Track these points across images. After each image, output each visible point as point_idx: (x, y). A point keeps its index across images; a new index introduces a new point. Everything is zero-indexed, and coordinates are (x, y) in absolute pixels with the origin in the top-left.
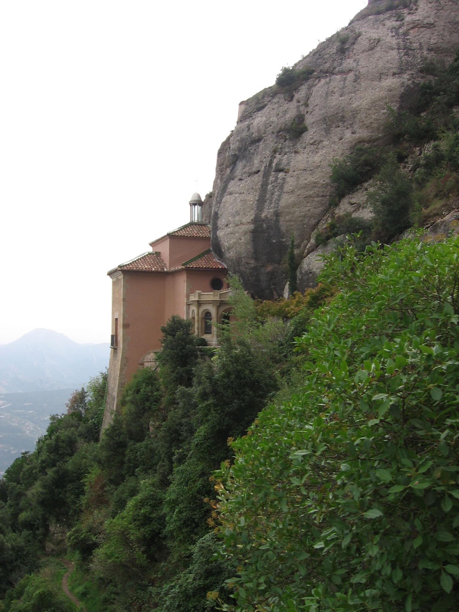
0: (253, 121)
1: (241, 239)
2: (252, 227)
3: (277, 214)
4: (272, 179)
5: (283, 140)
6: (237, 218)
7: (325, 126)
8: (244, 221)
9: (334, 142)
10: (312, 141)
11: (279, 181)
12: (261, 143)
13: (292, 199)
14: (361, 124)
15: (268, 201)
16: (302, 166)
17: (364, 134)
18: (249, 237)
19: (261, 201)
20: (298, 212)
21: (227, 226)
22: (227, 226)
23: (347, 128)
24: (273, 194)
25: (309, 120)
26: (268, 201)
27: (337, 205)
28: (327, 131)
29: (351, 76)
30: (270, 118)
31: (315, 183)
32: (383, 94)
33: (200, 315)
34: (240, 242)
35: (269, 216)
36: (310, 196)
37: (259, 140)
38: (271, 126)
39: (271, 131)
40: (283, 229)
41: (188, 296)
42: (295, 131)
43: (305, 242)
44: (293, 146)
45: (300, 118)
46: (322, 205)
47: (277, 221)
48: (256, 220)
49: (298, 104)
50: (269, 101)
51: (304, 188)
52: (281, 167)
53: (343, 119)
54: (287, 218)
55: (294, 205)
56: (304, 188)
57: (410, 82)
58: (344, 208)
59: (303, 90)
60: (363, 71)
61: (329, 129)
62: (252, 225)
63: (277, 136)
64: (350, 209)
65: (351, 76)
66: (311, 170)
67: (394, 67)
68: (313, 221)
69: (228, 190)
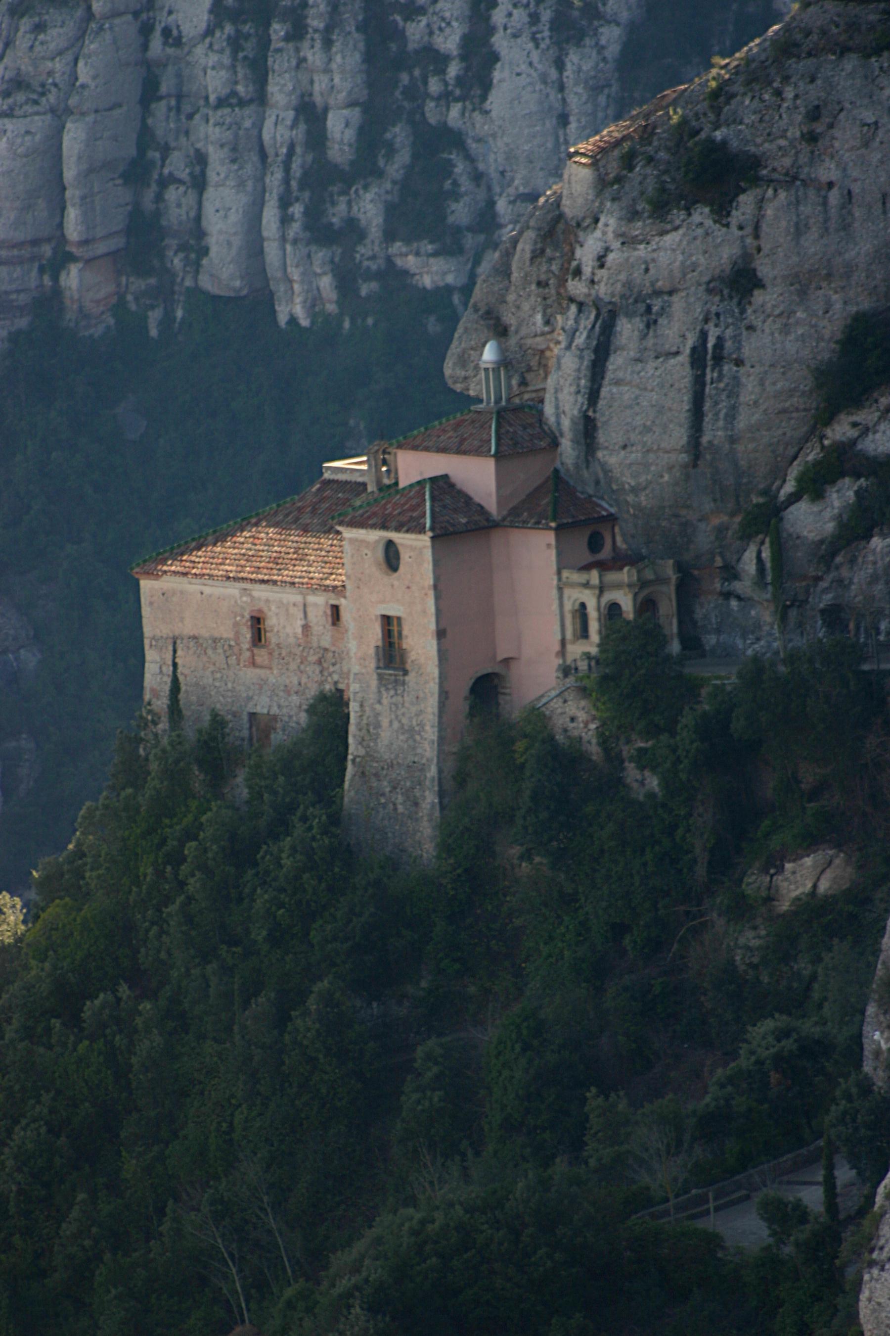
0: (655, 255)
1: (662, 476)
5: (717, 298)
6: (648, 438)
7: (797, 286)
10: (777, 312)
12: (675, 298)
21: (625, 447)
22: (625, 447)
24: (716, 403)
25: (764, 269)
26: (710, 415)
28: (803, 293)
29: (834, 198)
30: (691, 255)
33: (602, 610)
34: (661, 481)
35: (716, 442)
37: (671, 293)
38: (693, 271)
41: (559, 573)
42: (741, 282)
43: (778, 483)
45: (747, 257)
49: (740, 233)
50: (683, 221)
54: (751, 446)
58: (840, 430)
59: (746, 201)
62: (683, 455)
63: (709, 291)
66: (783, 367)
68: (792, 451)
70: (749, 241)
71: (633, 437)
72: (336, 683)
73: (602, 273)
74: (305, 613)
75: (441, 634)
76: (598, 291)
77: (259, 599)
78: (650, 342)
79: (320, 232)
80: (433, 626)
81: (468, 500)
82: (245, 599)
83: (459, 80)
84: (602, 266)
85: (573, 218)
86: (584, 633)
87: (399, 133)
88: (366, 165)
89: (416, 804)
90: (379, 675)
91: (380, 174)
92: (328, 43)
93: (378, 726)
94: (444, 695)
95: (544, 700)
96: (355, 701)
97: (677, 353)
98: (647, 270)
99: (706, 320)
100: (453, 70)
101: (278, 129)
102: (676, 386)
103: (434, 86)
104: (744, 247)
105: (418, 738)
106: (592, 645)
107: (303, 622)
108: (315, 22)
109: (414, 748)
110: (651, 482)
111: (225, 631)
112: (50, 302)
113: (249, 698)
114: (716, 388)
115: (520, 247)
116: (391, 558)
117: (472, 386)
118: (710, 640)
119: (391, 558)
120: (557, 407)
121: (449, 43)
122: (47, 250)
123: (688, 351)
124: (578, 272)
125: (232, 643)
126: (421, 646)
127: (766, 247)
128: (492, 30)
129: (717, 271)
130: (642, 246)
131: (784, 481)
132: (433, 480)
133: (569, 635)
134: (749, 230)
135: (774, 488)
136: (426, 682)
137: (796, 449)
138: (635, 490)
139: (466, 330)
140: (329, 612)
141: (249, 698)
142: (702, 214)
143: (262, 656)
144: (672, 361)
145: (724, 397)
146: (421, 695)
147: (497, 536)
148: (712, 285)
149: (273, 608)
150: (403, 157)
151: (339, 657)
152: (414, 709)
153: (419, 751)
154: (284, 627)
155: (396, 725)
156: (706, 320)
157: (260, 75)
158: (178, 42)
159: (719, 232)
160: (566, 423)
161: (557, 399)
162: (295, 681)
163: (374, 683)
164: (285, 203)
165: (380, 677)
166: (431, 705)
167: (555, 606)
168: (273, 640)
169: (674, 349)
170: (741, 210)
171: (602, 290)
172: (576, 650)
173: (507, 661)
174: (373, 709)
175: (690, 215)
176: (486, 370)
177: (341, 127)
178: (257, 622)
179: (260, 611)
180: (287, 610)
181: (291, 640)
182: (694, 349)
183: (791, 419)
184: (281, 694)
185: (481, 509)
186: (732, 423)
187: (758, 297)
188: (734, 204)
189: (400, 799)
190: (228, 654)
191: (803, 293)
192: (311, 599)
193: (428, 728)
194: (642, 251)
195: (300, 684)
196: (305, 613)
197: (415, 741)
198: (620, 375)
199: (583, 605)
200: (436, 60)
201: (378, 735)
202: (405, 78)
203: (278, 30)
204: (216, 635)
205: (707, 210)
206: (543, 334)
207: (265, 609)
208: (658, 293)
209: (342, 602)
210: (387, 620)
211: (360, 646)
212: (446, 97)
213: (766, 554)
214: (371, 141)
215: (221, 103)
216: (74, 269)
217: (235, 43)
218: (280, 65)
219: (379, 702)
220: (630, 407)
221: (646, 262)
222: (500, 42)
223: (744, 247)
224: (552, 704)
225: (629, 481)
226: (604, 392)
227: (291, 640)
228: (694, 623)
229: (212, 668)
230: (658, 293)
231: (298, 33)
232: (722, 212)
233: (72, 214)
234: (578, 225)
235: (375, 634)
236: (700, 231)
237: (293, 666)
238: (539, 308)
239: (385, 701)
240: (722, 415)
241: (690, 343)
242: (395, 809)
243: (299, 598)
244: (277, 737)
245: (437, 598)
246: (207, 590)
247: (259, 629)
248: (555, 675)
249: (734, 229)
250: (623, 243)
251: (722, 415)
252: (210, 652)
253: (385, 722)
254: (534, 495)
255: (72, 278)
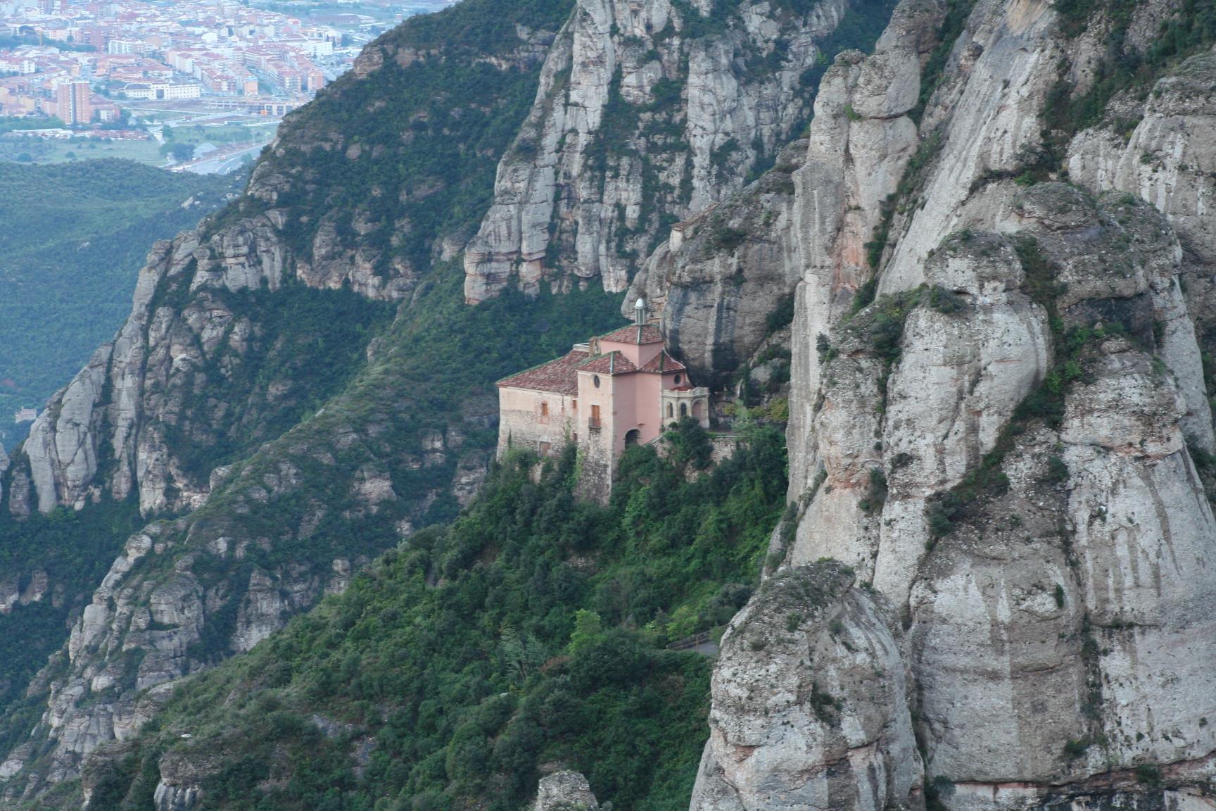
79: (621, 254)
81: (627, 361)
83: (679, 197)
87: (654, 216)
88: (639, 230)
91: (646, 231)
92: (628, 181)
100: (677, 192)
101: (607, 212)
103: (669, 198)
108: (623, 173)
112: (515, 277)
116: (597, 382)
119: (597, 382)
121: (676, 181)
122: (515, 257)
128: (692, 177)
147: (639, 377)
150: (656, 225)
151: (576, 421)
157: (601, 191)
158: (569, 177)
164: (608, 242)
177: (632, 212)
178: (544, 405)
185: (633, 365)
191: (762, 285)
200: (669, 188)
202: (657, 194)
203: (609, 174)
211: (583, 417)
212: (674, 202)
214: (643, 218)
215: (585, 202)
216: (525, 264)
217: (591, 179)
218: (610, 187)
222: (696, 182)
231: (616, 176)
233: (524, 244)
254: (653, 362)
255: (524, 268)
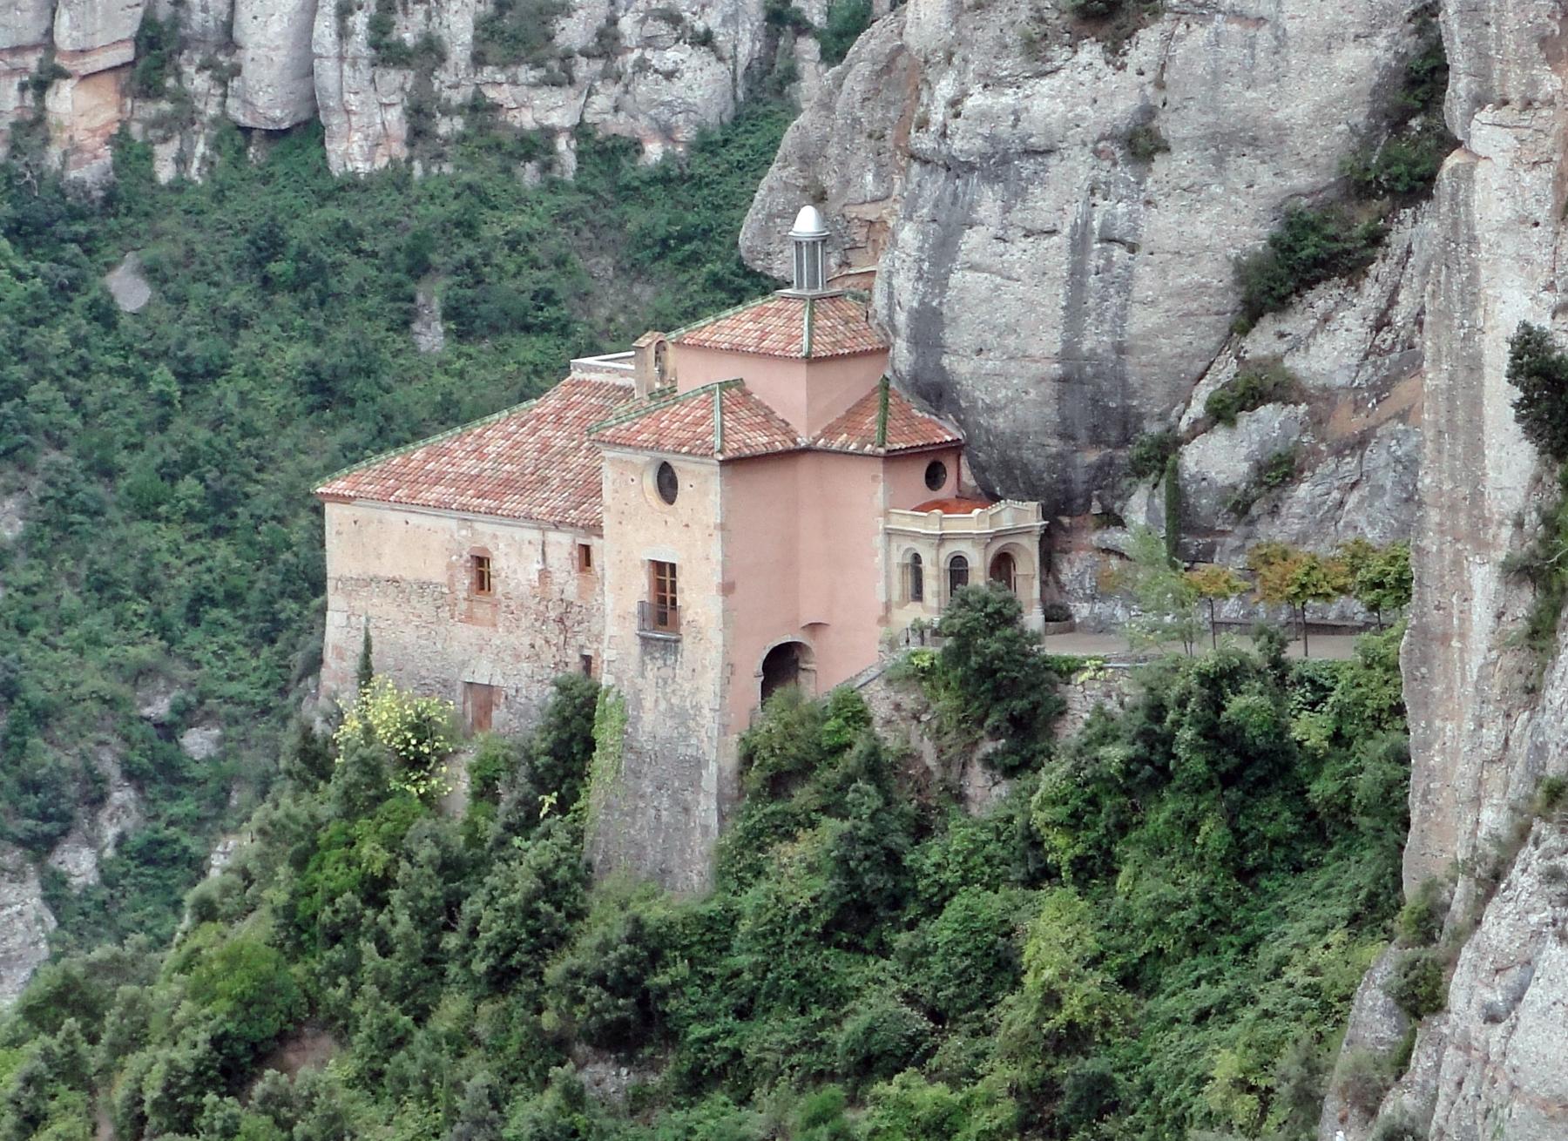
0: (1026, 103)
1: (1026, 393)
2: (1056, 369)
3: (1120, 349)
4: (1094, 261)
5: (1107, 164)
6: (1011, 341)
7: (1213, 151)
8: (1035, 350)
9: (1236, 192)
10: (1185, 184)
11: (1116, 271)
13: (1154, 319)
14: (1294, 159)
15: (1094, 315)
16: (1170, 243)
17: (1301, 179)
18: (1049, 390)
19: (1074, 312)
20: (1166, 346)
23: (1263, 162)
25: (1169, 127)
27: (1245, 331)
28: (1219, 161)
31: (1205, 286)
32: (1337, 88)
33: (942, 565)
34: (1026, 398)
35: (1099, 351)
36: (1190, 314)
37: (1048, 152)
39: (1078, 139)
40: (1134, 380)
42: (1140, 144)
43: (1181, 406)
44: (1138, 183)
45: (1149, 112)
46: (1217, 333)
47: (1120, 362)
48: (1067, 354)
51: (1179, 295)
52: (1116, 234)
53: (1254, 142)
55: (1158, 332)
56: (1179, 295)
57: (1390, 55)
58: (1262, 342)
60: (1292, 27)
61: (1223, 161)
63: (1097, 153)
64: (1280, 347)
65: (1264, 36)
67: (1353, 21)
68: (1200, 366)
69: (961, 257)
70: (1150, 90)
71: (990, 338)
72: (582, 647)
73: (953, 124)
74: (544, 553)
75: (727, 588)
76: (950, 147)
77: (483, 533)
78: (1016, 216)
80: (717, 579)
81: (769, 414)
82: (464, 532)
84: (957, 115)
85: (919, 51)
86: (918, 594)
89: (686, 810)
90: (643, 638)
93: (639, 704)
94: (730, 668)
95: (862, 681)
96: (609, 672)
97: (1053, 232)
98: (1017, 120)
99: (1092, 192)
102: (1050, 274)
104: (1145, 97)
105: (692, 724)
106: (931, 609)
107: (540, 567)
109: (686, 738)
110: (1012, 400)
111: (435, 572)
113: (464, 664)
114: (1101, 280)
115: (847, 84)
117: (776, 265)
118: (1082, 611)
120: (890, 296)
123: (1067, 230)
124: (923, 124)
125: (445, 590)
126: (699, 601)
127: (1174, 99)
129: (1108, 129)
130: (1010, 91)
131: (1188, 404)
132: (724, 386)
133: (896, 596)
134: (1150, 75)
135: (1174, 413)
136: (707, 650)
137: (1206, 363)
138: (990, 409)
139: (771, 189)
140: (576, 554)
141: (464, 664)
142: (1090, 52)
143: (482, 611)
144: (1047, 242)
145: (1112, 291)
146: (699, 669)
148: (1100, 146)
149: (501, 546)
152: (687, 686)
153: (693, 741)
154: (515, 572)
155: (663, 706)
156: (1092, 192)
159: (1111, 78)
160: (901, 318)
161: (890, 285)
162: (527, 641)
163: (636, 649)
165: (645, 641)
166: (710, 682)
167: (879, 559)
168: (498, 586)
169: (1048, 227)
170: (1142, 49)
171: (957, 144)
172: (908, 615)
173: (814, 627)
174: (633, 684)
175: (1076, 52)
176: (798, 244)
179: (485, 550)
180: (520, 549)
181: (525, 589)
182: (1075, 227)
183: (1199, 323)
184: (508, 659)
186: (1121, 327)
187: (1160, 165)
188: (1134, 40)
189: (666, 802)
190: (439, 603)
191: (1219, 161)
192: (553, 536)
193: (706, 711)
194: (1009, 98)
195: (533, 646)
196: (544, 553)
197: (688, 727)
198: (976, 257)
199: (917, 558)
201: (638, 718)
204: (425, 578)
205: (1098, 48)
206: (875, 201)
207: (490, 547)
208: (1030, 152)
209: (594, 542)
210: (659, 567)
213: (1160, 502)
219: (643, 676)
220: (988, 300)
221: (1015, 112)
223: (1145, 97)
224: (872, 685)
225: (982, 396)
226: (955, 279)
227: (525, 589)
228: (1060, 586)
229: (416, 621)
230: (1030, 152)
232: (1114, 52)
234: (926, 62)
235: (641, 587)
236: (1087, 76)
237: (525, 623)
238: (871, 166)
239: (649, 675)
240: (1109, 315)
241: (1069, 220)
242: (658, 818)
243: (535, 535)
244: (498, 715)
245: (725, 542)
246: (414, 519)
247: (482, 573)
248: (879, 647)
249: (1131, 71)
250: (986, 86)
251: (1109, 315)
252: (414, 602)
253: (648, 703)
